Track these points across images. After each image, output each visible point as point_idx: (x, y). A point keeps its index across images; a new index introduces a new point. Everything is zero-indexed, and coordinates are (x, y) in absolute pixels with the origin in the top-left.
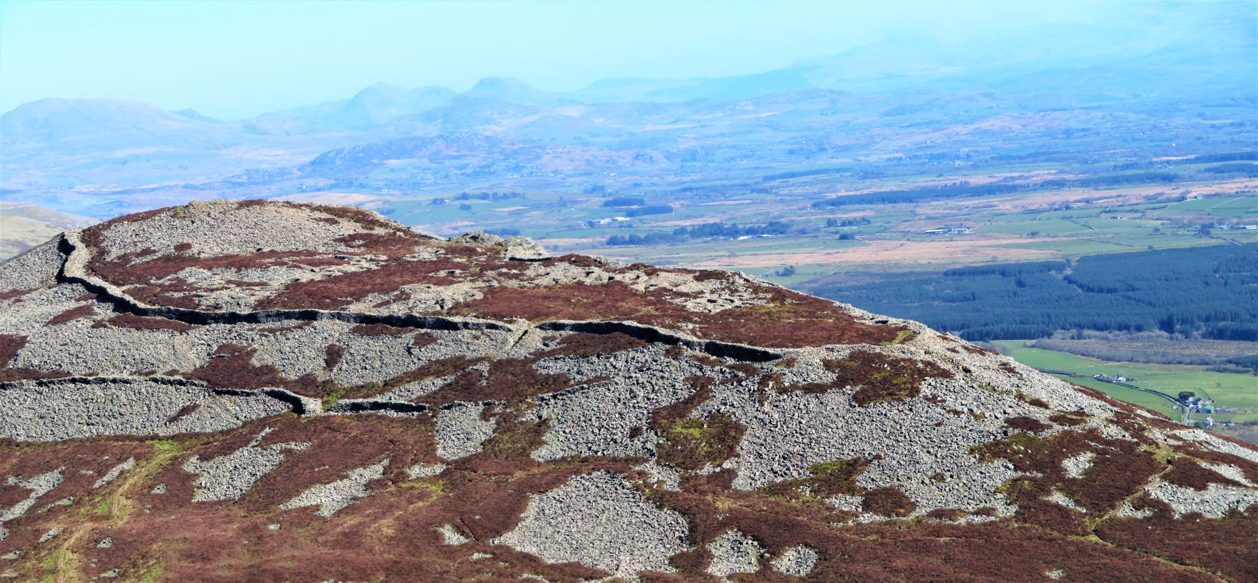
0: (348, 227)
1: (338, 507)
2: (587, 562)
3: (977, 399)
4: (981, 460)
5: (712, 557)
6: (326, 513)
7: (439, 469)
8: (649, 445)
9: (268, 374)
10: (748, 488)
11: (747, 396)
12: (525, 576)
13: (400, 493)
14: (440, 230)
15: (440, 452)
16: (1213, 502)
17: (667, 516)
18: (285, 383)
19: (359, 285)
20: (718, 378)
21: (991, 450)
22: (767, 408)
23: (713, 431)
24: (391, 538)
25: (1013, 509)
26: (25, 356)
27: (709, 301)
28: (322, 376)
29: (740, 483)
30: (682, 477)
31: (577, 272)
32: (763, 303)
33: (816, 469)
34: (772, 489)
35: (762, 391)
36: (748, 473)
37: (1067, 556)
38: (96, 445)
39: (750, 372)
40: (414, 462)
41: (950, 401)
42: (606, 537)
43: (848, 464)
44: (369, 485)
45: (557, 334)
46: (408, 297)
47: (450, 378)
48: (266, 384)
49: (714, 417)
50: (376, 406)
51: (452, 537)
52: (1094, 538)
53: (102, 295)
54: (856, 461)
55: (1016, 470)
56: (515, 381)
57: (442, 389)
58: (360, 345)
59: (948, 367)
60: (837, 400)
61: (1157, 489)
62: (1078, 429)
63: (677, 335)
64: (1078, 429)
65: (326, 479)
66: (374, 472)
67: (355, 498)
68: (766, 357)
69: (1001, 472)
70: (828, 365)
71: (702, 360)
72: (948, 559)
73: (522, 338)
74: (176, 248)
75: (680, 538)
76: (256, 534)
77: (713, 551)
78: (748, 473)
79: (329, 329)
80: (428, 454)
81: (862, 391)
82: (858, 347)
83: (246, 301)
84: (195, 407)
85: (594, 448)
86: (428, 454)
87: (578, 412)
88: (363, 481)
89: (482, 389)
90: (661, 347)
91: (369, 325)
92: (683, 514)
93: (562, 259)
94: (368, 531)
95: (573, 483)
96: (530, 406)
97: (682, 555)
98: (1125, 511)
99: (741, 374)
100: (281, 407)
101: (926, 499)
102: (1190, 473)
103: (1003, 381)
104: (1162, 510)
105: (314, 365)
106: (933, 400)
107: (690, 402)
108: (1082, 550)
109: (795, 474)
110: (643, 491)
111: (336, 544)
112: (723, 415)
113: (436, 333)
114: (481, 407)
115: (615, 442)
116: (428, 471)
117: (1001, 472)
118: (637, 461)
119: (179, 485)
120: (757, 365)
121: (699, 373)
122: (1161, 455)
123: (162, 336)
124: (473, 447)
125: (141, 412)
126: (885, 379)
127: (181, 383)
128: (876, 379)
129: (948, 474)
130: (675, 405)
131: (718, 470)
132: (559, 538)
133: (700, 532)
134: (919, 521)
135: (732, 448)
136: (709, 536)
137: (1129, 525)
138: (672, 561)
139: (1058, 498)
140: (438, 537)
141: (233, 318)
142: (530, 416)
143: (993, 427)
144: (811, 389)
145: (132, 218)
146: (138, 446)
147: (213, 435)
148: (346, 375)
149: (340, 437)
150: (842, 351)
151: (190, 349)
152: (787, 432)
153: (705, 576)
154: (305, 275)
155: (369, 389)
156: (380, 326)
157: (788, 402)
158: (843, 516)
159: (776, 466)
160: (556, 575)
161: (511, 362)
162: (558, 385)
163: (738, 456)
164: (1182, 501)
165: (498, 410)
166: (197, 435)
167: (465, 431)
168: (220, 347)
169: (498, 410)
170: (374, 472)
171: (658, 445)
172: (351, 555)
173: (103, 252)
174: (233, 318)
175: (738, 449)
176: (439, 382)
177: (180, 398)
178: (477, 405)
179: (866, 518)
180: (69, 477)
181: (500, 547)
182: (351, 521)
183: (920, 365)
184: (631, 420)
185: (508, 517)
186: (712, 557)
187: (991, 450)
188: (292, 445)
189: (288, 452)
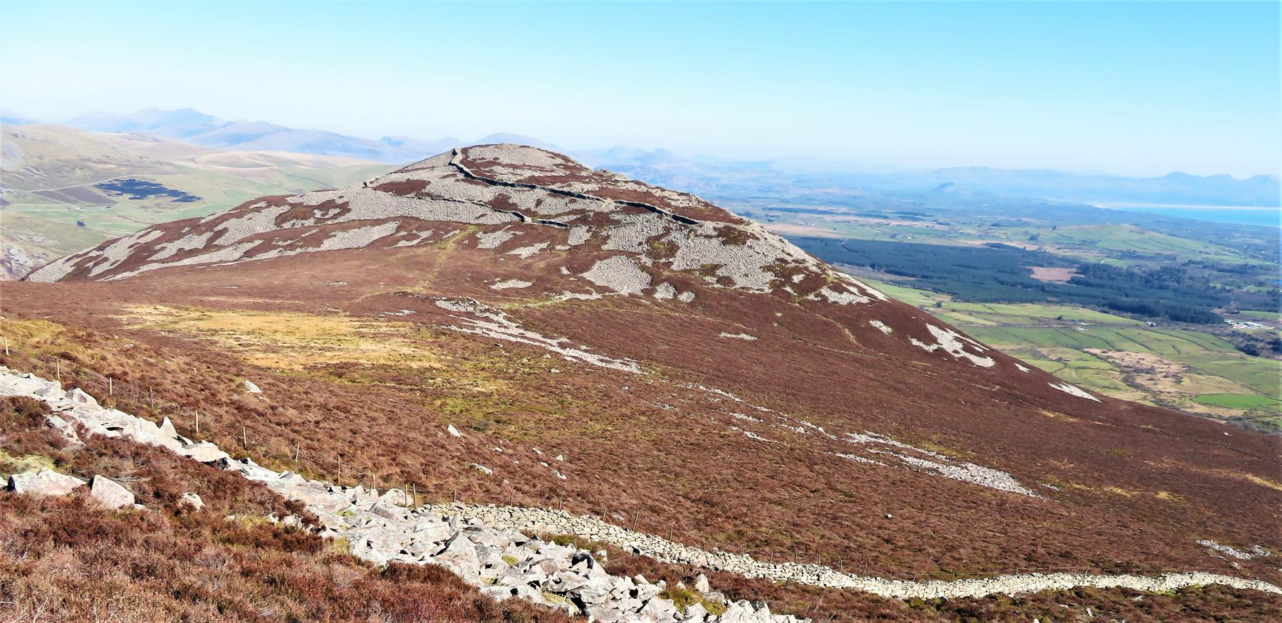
0: (559, 161)
14: (591, 165)
16: (844, 299)
19: (555, 180)
21: (767, 268)
26: (428, 189)
27: (682, 203)
29: (674, 267)
31: (636, 187)
32: (700, 207)
34: (685, 271)
36: (678, 264)
38: (448, 223)
49: (670, 242)
51: (565, 271)
53: (461, 170)
56: (602, 220)
60: (715, 242)
61: (825, 291)
66: (544, 245)
68: (693, 223)
69: (770, 276)
70: (715, 229)
73: (608, 205)
76: (495, 260)
78: (678, 264)
79: (539, 193)
80: (565, 242)
83: (513, 179)
86: (565, 242)
91: (555, 193)
98: (811, 297)
100: (517, 219)
101: (740, 282)
102: (838, 287)
103: (779, 245)
104: (825, 299)
105: (532, 206)
106: (750, 247)
107: (662, 236)
108: (791, 308)
117: (770, 276)
119: (474, 240)
122: (829, 280)
123: (479, 187)
124: (582, 242)
125: (467, 214)
128: (732, 236)
133: (655, 282)
136: (658, 283)
137: (811, 302)
139: (788, 289)
140: (559, 270)
141: (506, 184)
142: (604, 233)
143: (770, 260)
146: (463, 226)
148: (542, 211)
150: (721, 225)
151: (489, 193)
152: (694, 251)
154: (537, 174)
155: (550, 216)
157: (697, 240)
164: (833, 296)
167: (580, 235)
170: (544, 245)
174: (506, 184)
177: (481, 210)
179: (716, 286)
180: (435, 233)
185: (587, 267)
187: (767, 268)
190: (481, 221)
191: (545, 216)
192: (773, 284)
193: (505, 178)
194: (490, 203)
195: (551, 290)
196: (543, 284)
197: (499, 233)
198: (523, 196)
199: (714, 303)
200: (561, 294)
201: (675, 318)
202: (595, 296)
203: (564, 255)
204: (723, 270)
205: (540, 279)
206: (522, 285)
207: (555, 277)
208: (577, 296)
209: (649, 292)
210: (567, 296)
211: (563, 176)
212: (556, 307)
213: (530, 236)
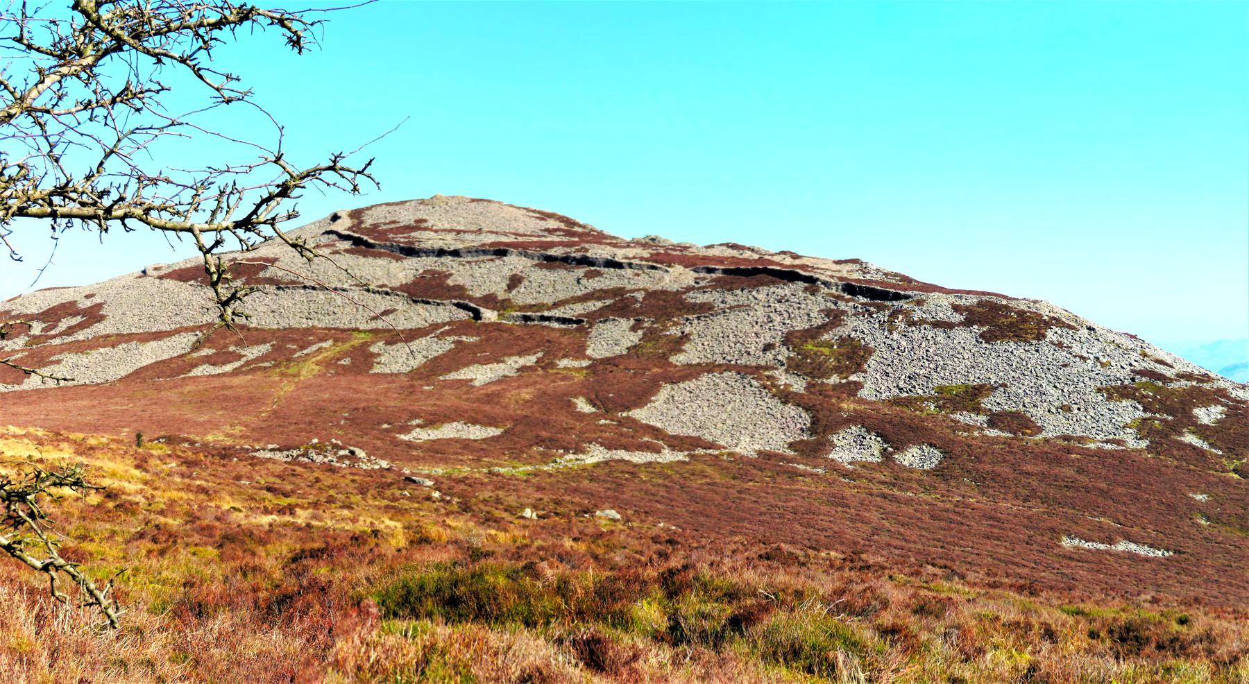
0: (552, 224)
1: (488, 380)
2: (710, 438)
3: (1103, 350)
4: (1110, 398)
5: (834, 446)
6: (477, 384)
7: (585, 363)
8: (780, 357)
9: (459, 290)
10: (874, 398)
11: (877, 326)
12: (646, 439)
13: (546, 376)
15: (589, 352)
17: (791, 410)
18: (471, 298)
20: (851, 312)
22: (895, 336)
23: (842, 350)
24: (527, 401)
25: (1144, 444)
28: (501, 295)
29: (866, 393)
30: (809, 383)
33: (941, 390)
34: (897, 401)
35: (891, 322)
36: (874, 386)
37: (1208, 484)
39: (880, 308)
40: (565, 356)
41: (1076, 349)
42: (728, 422)
43: (974, 388)
44: (522, 369)
45: (708, 276)
46: (587, 250)
47: (608, 302)
48: (455, 298)
49: (843, 341)
50: (543, 318)
51: (583, 406)
52: (1236, 476)
54: (982, 386)
55: (1145, 410)
56: (668, 305)
57: (601, 309)
58: (539, 275)
59: (1073, 324)
60: (964, 337)
62: (1207, 386)
63: (817, 276)
64: (1207, 386)
65: (487, 361)
66: (530, 360)
67: (505, 376)
69: (1129, 412)
70: (956, 308)
71: (838, 297)
72: (1080, 471)
73: (676, 278)
74: (416, 221)
75: (802, 429)
77: (836, 441)
78: (874, 386)
79: (516, 263)
80: (579, 352)
81: (989, 331)
82: (985, 298)
84: (395, 310)
85: (729, 358)
86: (579, 352)
87: (719, 329)
88: (517, 366)
89: (635, 309)
90: (801, 285)
91: (550, 262)
92: (807, 409)
93: (722, 245)
94: (508, 394)
95: (705, 379)
96: (676, 324)
97: (802, 441)
99: (872, 309)
100: (463, 315)
101: (1053, 427)
107: (823, 328)
108: (1226, 482)
109: (920, 392)
110: (770, 390)
111: (478, 400)
112: (853, 339)
113: (603, 270)
114: (632, 322)
115: (749, 354)
116: (576, 364)
118: (767, 368)
120: (888, 303)
121: (833, 307)
124: (620, 350)
126: (1011, 324)
127: (387, 293)
129: (1075, 407)
130: (808, 330)
131: (844, 381)
132: (684, 419)
133: (823, 425)
134: (1047, 441)
135: (859, 365)
138: (791, 446)
139: (1190, 439)
140: (571, 405)
141: (441, 253)
142: (674, 331)
143: (1120, 372)
144: (937, 324)
145: (387, 204)
147: (402, 332)
148: (522, 296)
149: (506, 335)
153: (826, 460)
156: (557, 263)
157: (916, 334)
158: (968, 428)
159: (901, 384)
160: (675, 443)
161: (664, 292)
162: (704, 310)
163: (866, 372)
165: (646, 325)
166: (390, 331)
168: (425, 272)
169: (646, 325)
170: (530, 360)
171: (789, 358)
172: (487, 408)
173: (362, 222)
175: (866, 366)
176: (599, 304)
177: (383, 303)
178: (628, 319)
179: (993, 433)
181: (628, 417)
182: (494, 388)
183: (1045, 318)
184: (767, 338)
185: (642, 397)
186: (834, 446)
188: (464, 338)
189: (460, 342)
190: (380, 324)
191: (531, 307)
192: (1143, 428)
193: (438, 244)
194: (404, 288)
195: (552, 443)
196: (534, 430)
197: (422, 342)
198: (478, 271)
199: (1004, 470)
200: (578, 450)
201: (908, 502)
202: (668, 456)
203: (579, 377)
204: (999, 396)
205: (517, 421)
206: (477, 433)
207: (563, 419)
208: (622, 454)
209: (814, 445)
210: (595, 455)
211: (569, 248)
212: (570, 475)
213: (495, 344)
